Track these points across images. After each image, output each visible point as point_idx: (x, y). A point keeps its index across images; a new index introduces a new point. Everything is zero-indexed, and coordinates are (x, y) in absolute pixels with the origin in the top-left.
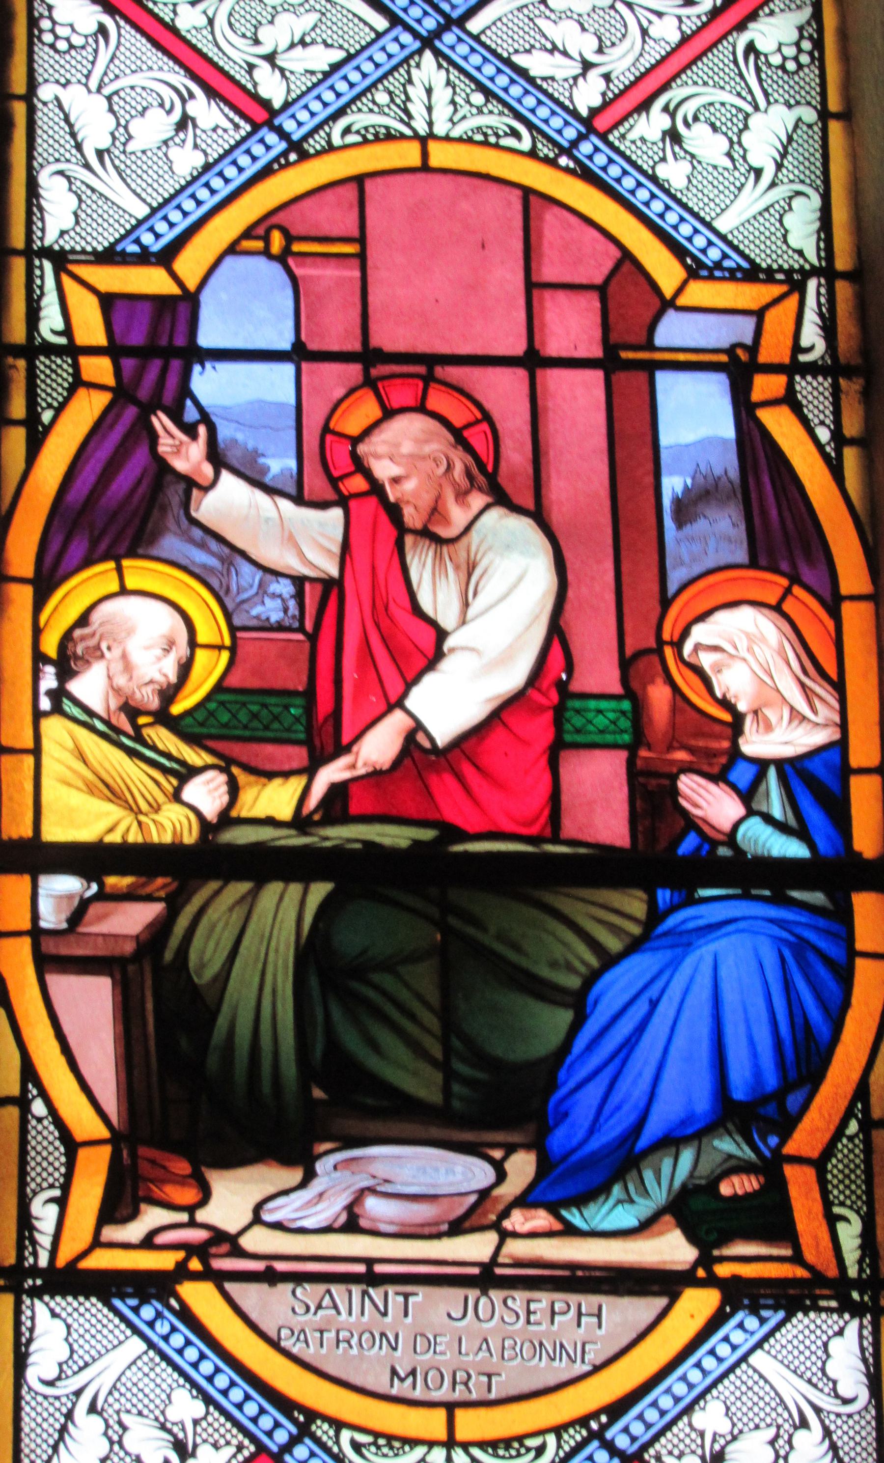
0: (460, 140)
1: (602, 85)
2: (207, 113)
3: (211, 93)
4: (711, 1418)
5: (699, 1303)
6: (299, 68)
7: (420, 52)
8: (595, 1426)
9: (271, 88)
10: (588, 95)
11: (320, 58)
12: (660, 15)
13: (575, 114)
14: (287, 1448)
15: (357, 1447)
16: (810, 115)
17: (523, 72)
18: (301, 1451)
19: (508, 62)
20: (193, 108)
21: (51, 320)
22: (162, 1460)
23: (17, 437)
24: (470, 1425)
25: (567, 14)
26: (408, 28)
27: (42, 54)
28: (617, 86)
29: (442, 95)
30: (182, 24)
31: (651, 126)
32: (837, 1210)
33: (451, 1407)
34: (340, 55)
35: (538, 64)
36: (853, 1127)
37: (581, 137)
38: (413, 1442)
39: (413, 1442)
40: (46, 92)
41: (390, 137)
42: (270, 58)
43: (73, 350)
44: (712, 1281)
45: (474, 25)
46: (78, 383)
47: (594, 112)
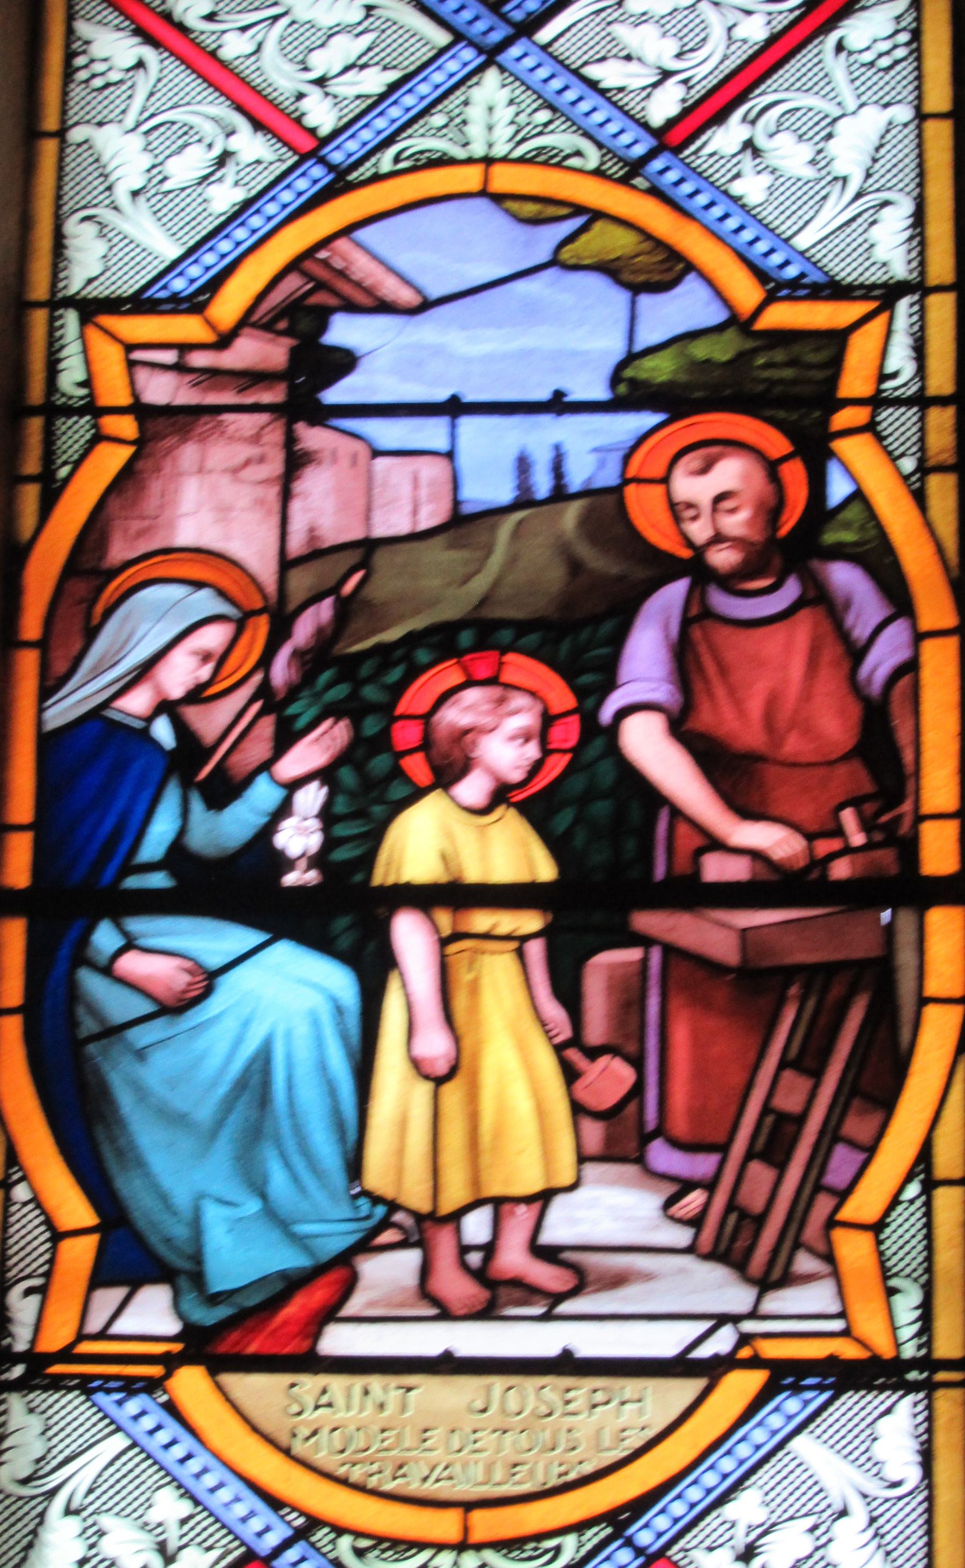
0: (522, 160)
1: (680, 92)
2: (251, 146)
3: (258, 125)
4: (746, 1509)
5: (741, 1385)
6: (352, 91)
7: (480, 69)
8: (620, 1519)
9: (321, 115)
10: (664, 106)
11: (374, 81)
12: (749, 13)
13: (645, 126)
14: (278, 1551)
15: (360, 1553)
16: (903, 113)
17: (593, 84)
18: (292, 1555)
19: (576, 73)
20: (234, 143)
21: (71, 376)
22: (142, 1565)
23: (30, 495)
24: (486, 1524)
25: (643, 19)
26: (471, 44)
27: (77, 93)
28: (696, 94)
29: (504, 114)
30: (226, 53)
31: (726, 138)
32: (893, 1282)
33: (468, 1506)
34: (393, 76)
35: (609, 74)
36: (913, 1189)
37: (651, 155)
38: (420, 1545)
39: (420, 1545)
40: (76, 135)
41: (443, 161)
42: (321, 82)
43: (92, 408)
44: (755, 1362)
45: (545, 35)
46: (98, 438)
47: (671, 123)
